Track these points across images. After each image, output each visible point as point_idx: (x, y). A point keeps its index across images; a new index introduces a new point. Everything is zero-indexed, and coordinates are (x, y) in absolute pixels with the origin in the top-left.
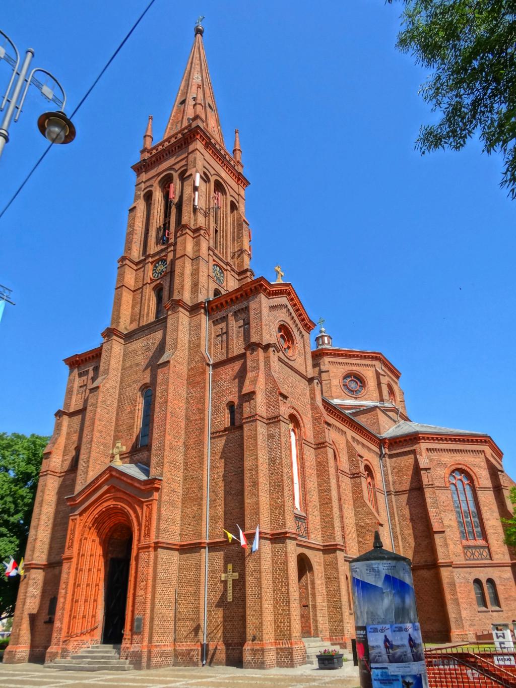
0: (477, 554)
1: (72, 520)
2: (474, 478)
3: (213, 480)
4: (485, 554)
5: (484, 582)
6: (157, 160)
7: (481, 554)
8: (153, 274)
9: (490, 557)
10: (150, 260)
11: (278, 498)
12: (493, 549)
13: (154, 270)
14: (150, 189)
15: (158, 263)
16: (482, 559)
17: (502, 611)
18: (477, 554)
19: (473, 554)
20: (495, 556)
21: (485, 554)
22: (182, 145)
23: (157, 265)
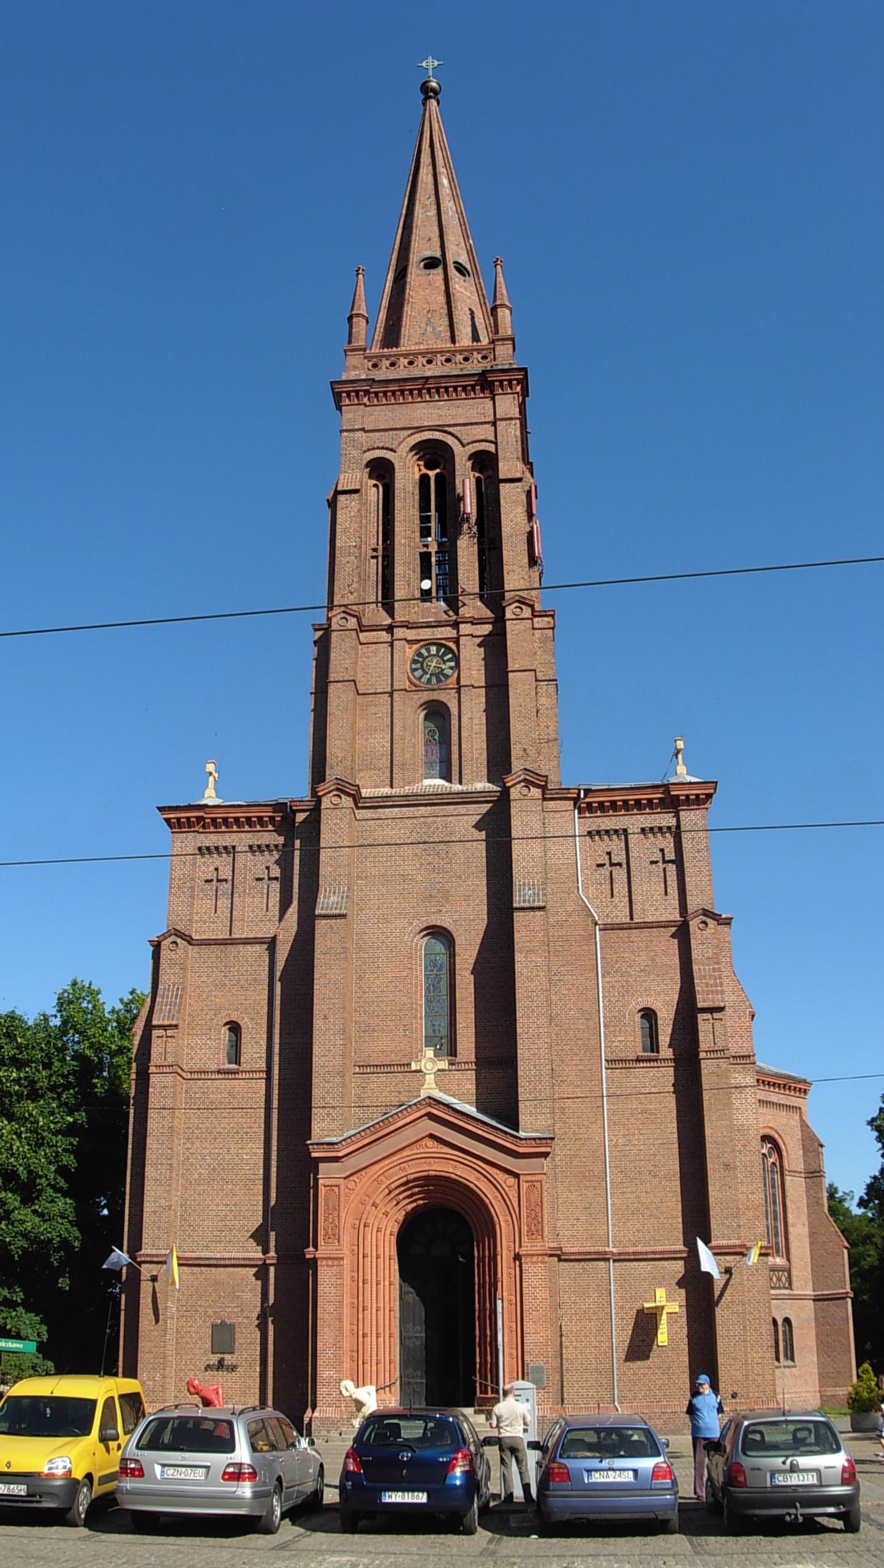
2: (784, 1153)
3: (616, 1146)
4: (783, 1279)
5: (780, 1322)
6: (402, 392)
7: (779, 1279)
8: (413, 670)
9: (790, 1284)
10: (411, 634)
11: (753, 1193)
12: (794, 1272)
13: (414, 662)
14: (388, 455)
15: (428, 651)
16: (779, 1288)
17: (795, 1367)
20: (795, 1284)
21: (783, 1279)
22: (473, 387)
23: (426, 654)
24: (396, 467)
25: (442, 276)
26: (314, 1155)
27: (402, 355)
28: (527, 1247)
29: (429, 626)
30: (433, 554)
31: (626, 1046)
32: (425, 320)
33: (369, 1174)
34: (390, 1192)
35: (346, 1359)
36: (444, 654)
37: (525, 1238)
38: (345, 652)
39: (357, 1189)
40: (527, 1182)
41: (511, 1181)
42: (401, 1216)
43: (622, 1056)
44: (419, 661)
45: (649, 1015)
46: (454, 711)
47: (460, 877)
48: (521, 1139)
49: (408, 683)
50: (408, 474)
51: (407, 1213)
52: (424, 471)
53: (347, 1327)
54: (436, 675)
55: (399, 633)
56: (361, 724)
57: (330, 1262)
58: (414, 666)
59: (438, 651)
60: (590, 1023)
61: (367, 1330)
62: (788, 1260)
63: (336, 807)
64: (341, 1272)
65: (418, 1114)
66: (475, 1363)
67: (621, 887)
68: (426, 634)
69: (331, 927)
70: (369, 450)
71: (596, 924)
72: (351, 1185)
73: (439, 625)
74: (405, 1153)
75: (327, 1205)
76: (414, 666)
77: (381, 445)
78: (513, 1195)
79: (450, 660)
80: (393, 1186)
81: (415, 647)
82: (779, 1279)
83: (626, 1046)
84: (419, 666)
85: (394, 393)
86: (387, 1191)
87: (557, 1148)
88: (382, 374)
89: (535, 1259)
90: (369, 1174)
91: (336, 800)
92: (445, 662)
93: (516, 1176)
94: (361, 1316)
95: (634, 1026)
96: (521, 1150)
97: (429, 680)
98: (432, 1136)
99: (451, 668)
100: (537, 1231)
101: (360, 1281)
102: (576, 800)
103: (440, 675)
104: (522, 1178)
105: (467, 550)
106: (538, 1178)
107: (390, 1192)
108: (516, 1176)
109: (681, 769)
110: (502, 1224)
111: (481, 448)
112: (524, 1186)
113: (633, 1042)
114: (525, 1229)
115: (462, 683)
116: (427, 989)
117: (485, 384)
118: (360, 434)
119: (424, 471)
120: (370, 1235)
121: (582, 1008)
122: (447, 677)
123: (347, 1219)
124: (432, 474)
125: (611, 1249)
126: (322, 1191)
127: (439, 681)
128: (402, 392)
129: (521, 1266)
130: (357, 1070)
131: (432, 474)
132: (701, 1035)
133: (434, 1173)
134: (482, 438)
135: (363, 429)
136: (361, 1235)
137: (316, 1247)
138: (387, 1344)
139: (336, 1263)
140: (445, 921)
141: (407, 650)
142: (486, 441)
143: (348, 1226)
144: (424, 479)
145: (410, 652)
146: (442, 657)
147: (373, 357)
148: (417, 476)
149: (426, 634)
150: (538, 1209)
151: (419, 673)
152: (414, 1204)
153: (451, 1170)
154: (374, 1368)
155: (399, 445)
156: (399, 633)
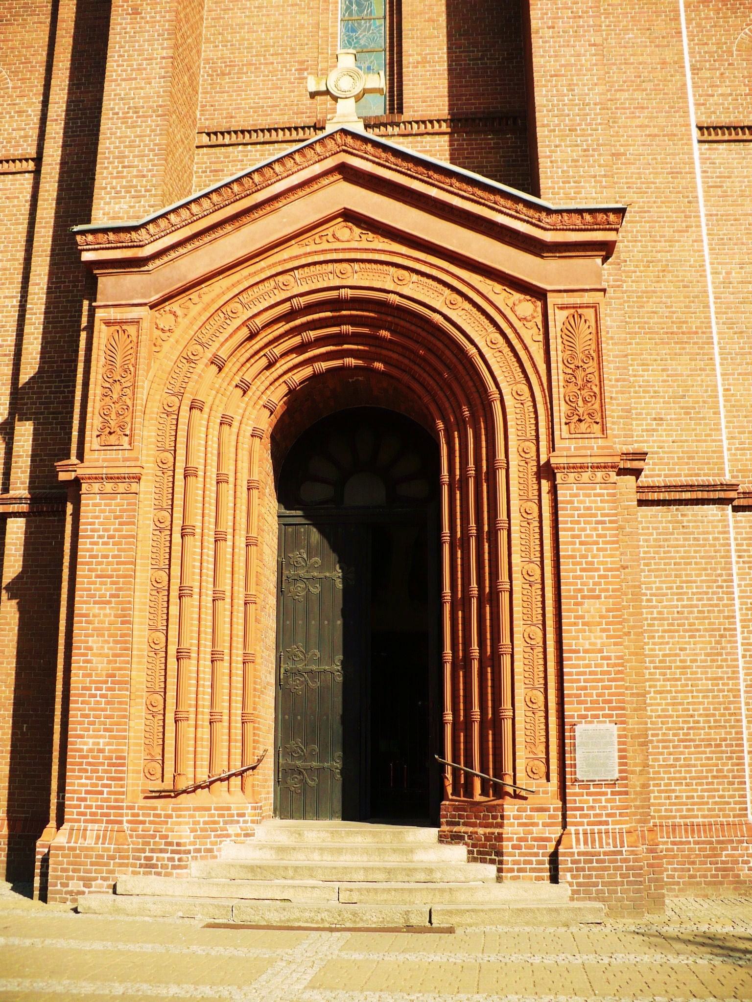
1: (108, 323)
3: (727, 283)
26: (86, 256)
28: (568, 449)
33: (206, 299)
34: (252, 336)
35: (138, 711)
39: (178, 332)
40: (562, 308)
41: (527, 307)
42: (278, 395)
48: (549, 211)
51: (290, 392)
53: (141, 634)
57: (109, 487)
61: (189, 642)
64: (133, 509)
65: (318, 169)
66: (442, 725)
72: (164, 319)
74: (286, 254)
75: (111, 362)
78: (532, 335)
80: (259, 321)
86: (244, 333)
87: (627, 239)
89: (586, 476)
90: (206, 299)
93: (538, 294)
94: (174, 610)
96: (548, 237)
98: (349, 216)
100: (592, 410)
101: (174, 531)
104: (552, 299)
106: (587, 298)
107: (252, 336)
108: (538, 294)
110: (509, 401)
112: (558, 318)
114: (561, 409)
120: (202, 430)
123: (151, 390)
126: (102, 333)
129: (554, 491)
130: (205, 140)
133: (350, 293)
136: (182, 427)
137: (81, 456)
138: (238, 680)
139: (122, 487)
143: (155, 408)
150: (592, 366)
152: (307, 371)
153: (390, 286)
154: (204, 732)
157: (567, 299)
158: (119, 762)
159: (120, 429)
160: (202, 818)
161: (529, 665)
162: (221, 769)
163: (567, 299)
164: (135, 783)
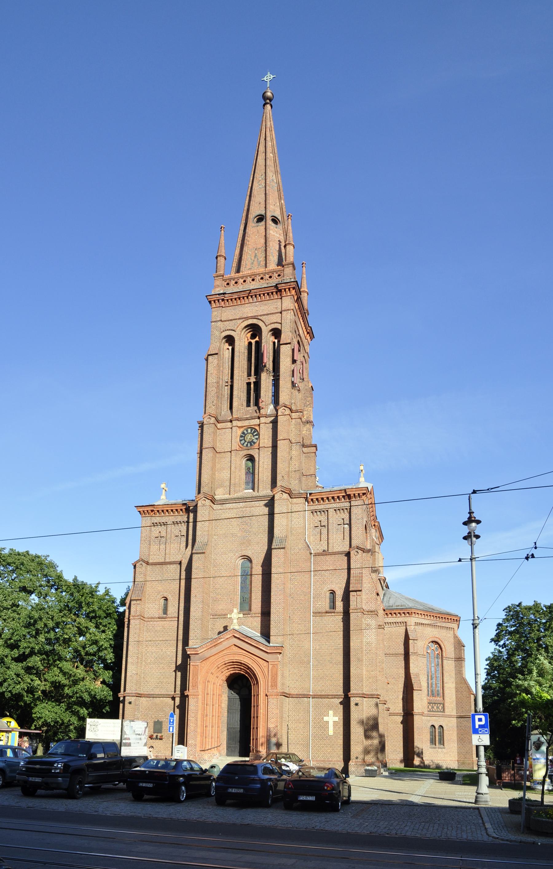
0: (435, 707)
3: (315, 649)
4: (440, 708)
7: (438, 708)
8: (241, 440)
9: (444, 710)
10: (239, 424)
12: (446, 705)
13: (241, 436)
15: (247, 431)
16: (438, 712)
18: (435, 707)
19: (433, 707)
20: (446, 710)
21: (440, 708)
23: (246, 433)
24: (236, 339)
25: (264, 227)
27: (240, 277)
29: (247, 419)
30: (252, 383)
31: (322, 607)
32: (254, 255)
35: (199, 736)
36: (254, 432)
37: (270, 688)
38: (209, 434)
43: (320, 611)
44: (243, 436)
45: (333, 593)
46: (257, 459)
47: (255, 534)
49: (238, 447)
50: (243, 340)
52: (250, 340)
53: (199, 723)
54: (250, 442)
55: (235, 423)
56: (218, 466)
58: (241, 439)
59: (251, 431)
60: (306, 597)
61: (208, 724)
62: (443, 699)
63: (204, 505)
67: (324, 536)
68: (246, 423)
69: (199, 558)
70: (224, 331)
71: (311, 554)
73: (252, 418)
76: (241, 439)
77: (229, 328)
79: (256, 435)
81: (242, 430)
82: (438, 708)
83: (322, 607)
84: (243, 438)
85: (235, 299)
88: (230, 290)
91: (203, 502)
92: (254, 436)
95: (326, 598)
97: (247, 445)
99: (257, 439)
101: (205, 704)
102: (306, 499)
103: (252, 443)
105: (266, 380)
109: (362, 479)
111: (274, 327)
113: (325, 605)
115: (261, 446)
116: (241, 583)
117: (278, 290)
118: (219, 323)
119: (250, 340)
120: (210, 686)
121: (302, 592)
122: (254, 443)
124: (253, 341)
125: (311, 693)
127: (251, 445)
128: (239, 298)
130: (212, 617)
131: (253, 341)
132: (351, 602)
134: (275, 321)
135: (221, 320)
138: (216, 731)
140: (249, 554)
141: (238, 431)
142: (277, 323)
144: (250, 344)
145: (239, 432)
146: (253, 434)
147: (226, 280)
148: (247, 343)
149: (246, 423)
151: (243, 442)
154: (210, 740)
155: (237, 327)
156: (235, 423)
157: (272, 663)
158: (195, 745)
159: (195, 686)
160: (209, 755)
161: (263, 730)
162: (213, 747)
163: (272, 663)
164: (198, 749)
